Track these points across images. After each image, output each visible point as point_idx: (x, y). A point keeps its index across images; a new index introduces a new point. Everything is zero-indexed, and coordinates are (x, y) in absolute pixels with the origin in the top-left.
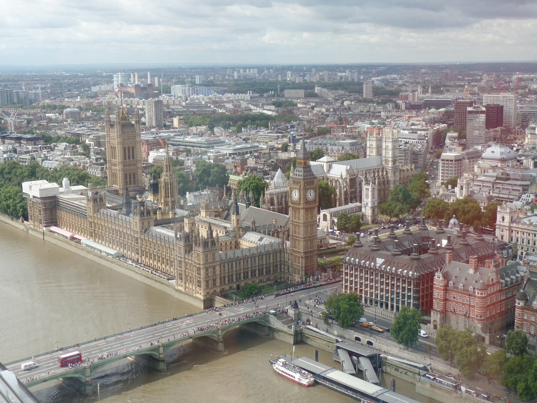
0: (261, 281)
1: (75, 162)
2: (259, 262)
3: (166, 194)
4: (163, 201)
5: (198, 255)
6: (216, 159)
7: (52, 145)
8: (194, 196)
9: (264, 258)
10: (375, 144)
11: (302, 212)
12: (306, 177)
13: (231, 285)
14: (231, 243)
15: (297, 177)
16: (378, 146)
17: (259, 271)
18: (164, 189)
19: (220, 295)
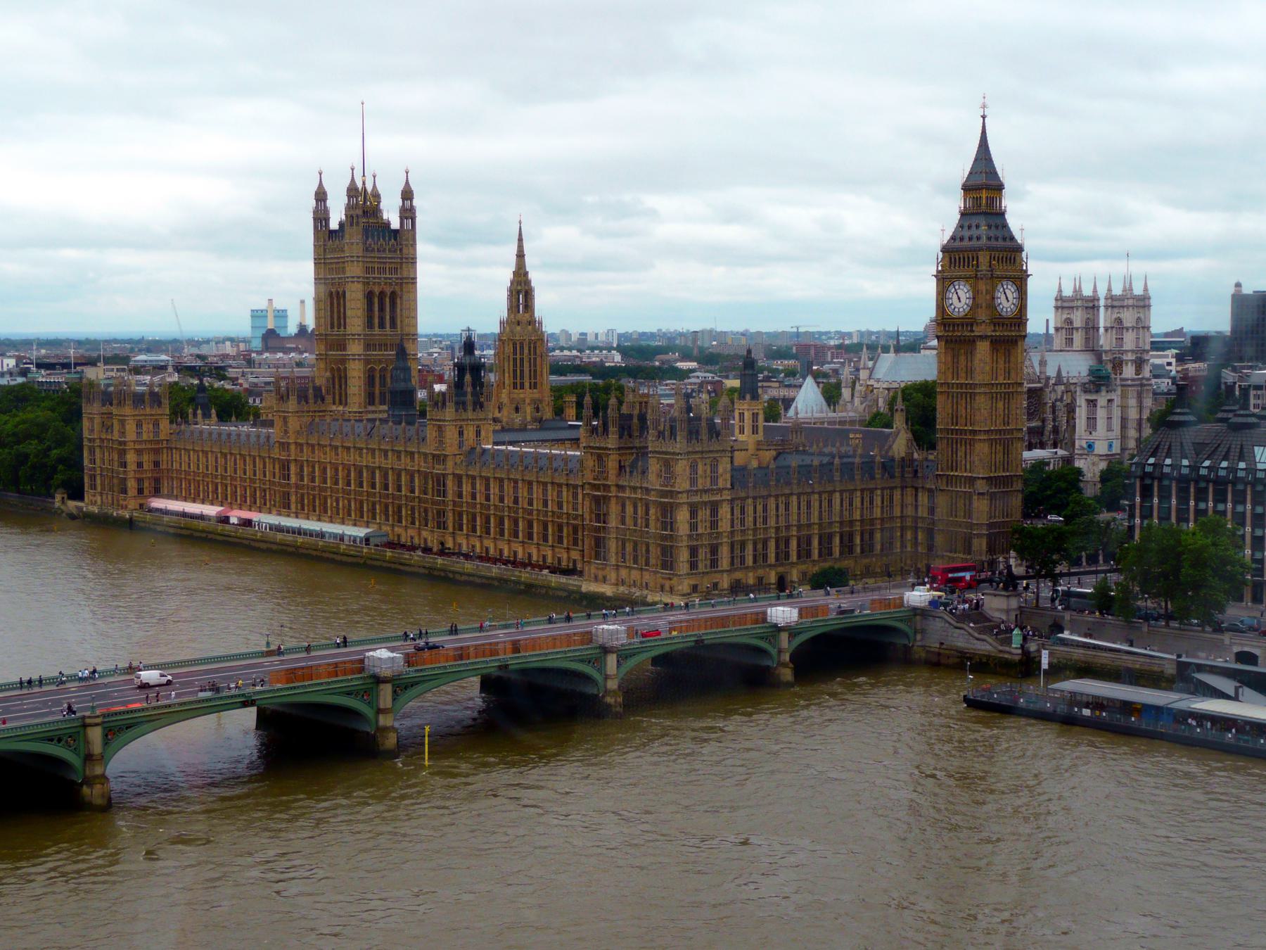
2: (841, 511)
3: (515, 377)
5: (667, 465)
9: (857, 502)
10: (1079, 319)
11: (983, 348)
12: (993, 243)
13: (760, 572)
15: (966, 243)
16: (1087, 323)
18: (511, 363)
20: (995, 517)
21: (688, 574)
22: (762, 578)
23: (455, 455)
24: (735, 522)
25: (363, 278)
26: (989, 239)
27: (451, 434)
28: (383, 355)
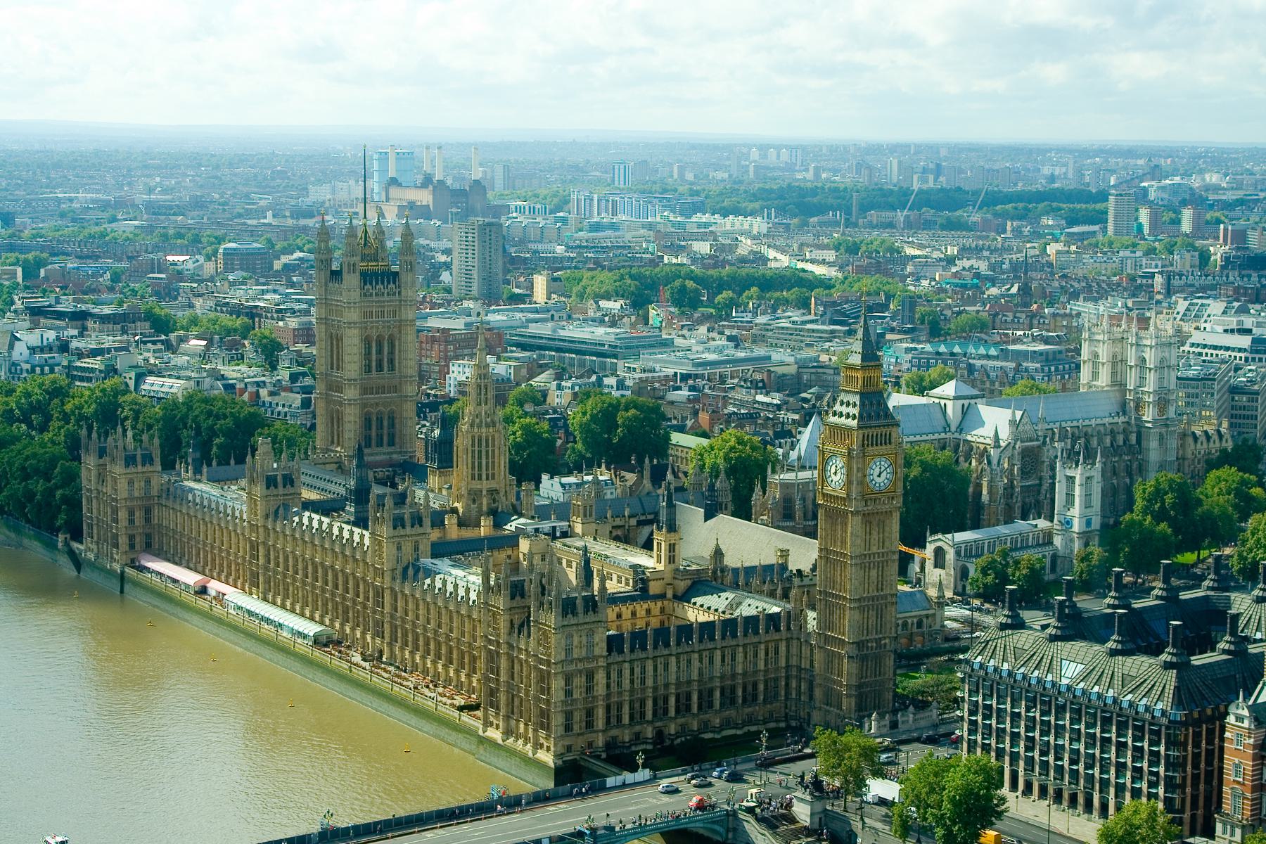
0: (727, 724)
1: (231, 382)
3: (473, 468)
4: (464, 491)
6: (640, 388)
7: (172, 336)
8: (563, 486)
13: (637, 728)
14: (648, 611)
16: (1114, 356)
17: (722, 694)
18: (470, 455)
19: (604, 756)
20: (866, 677)
21: (562, 736)
22: (639, 733)
23: (393, 570)
24: (612, 685)
25: (361, 323)
26: (861, 417)
27: (388, 550)
28: (380, 398)
